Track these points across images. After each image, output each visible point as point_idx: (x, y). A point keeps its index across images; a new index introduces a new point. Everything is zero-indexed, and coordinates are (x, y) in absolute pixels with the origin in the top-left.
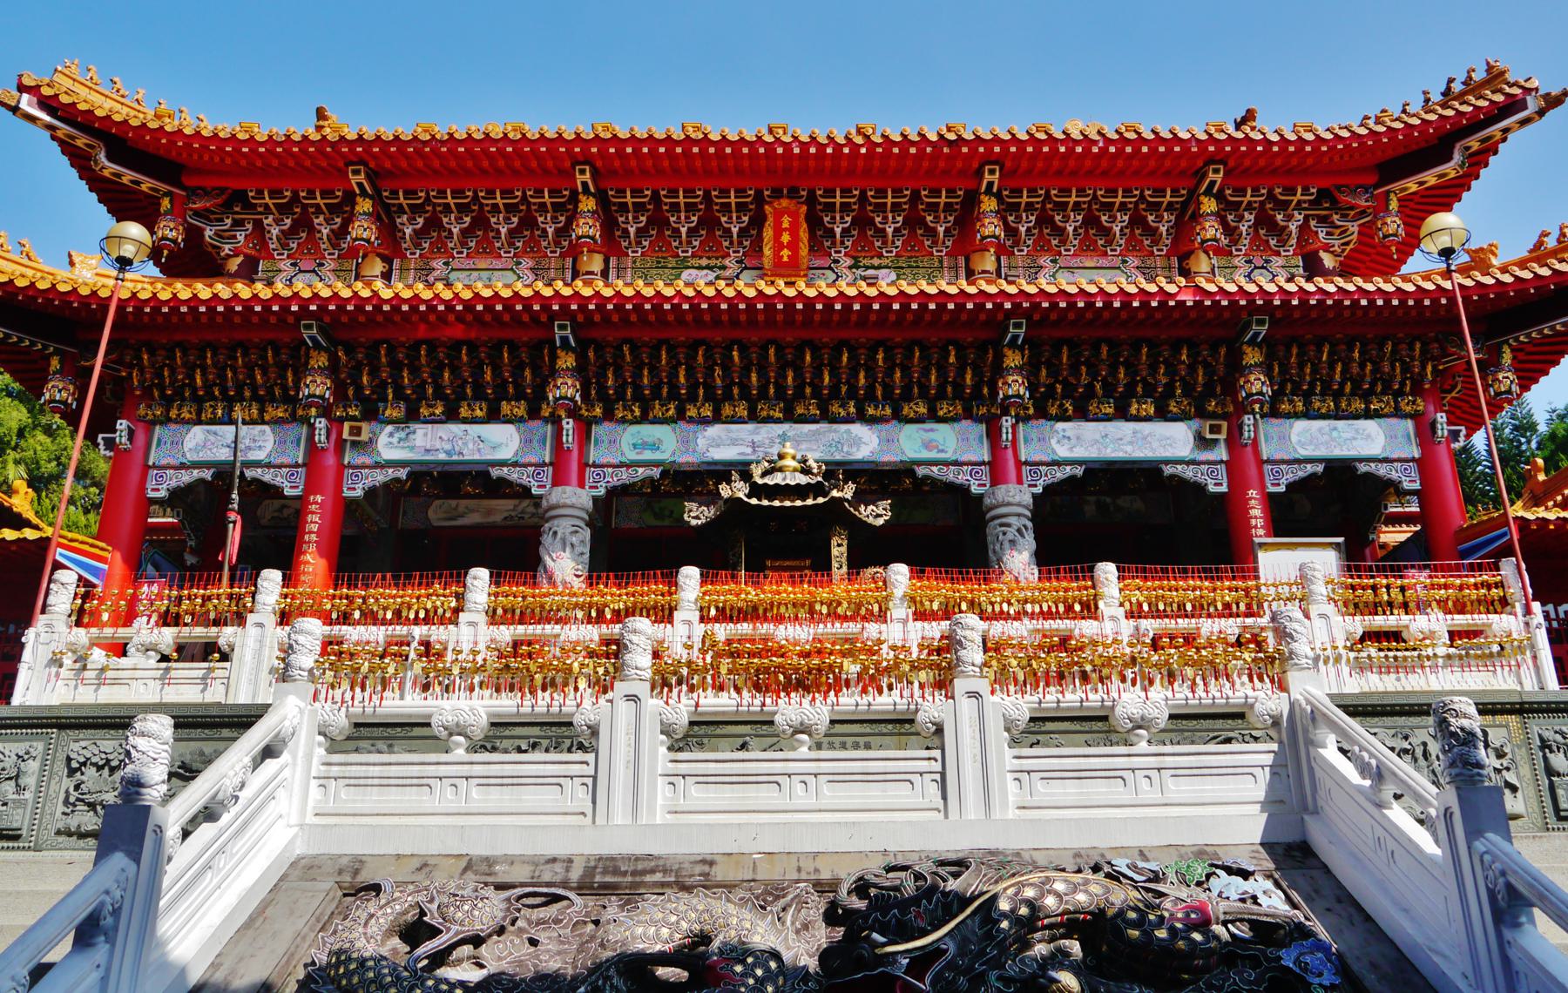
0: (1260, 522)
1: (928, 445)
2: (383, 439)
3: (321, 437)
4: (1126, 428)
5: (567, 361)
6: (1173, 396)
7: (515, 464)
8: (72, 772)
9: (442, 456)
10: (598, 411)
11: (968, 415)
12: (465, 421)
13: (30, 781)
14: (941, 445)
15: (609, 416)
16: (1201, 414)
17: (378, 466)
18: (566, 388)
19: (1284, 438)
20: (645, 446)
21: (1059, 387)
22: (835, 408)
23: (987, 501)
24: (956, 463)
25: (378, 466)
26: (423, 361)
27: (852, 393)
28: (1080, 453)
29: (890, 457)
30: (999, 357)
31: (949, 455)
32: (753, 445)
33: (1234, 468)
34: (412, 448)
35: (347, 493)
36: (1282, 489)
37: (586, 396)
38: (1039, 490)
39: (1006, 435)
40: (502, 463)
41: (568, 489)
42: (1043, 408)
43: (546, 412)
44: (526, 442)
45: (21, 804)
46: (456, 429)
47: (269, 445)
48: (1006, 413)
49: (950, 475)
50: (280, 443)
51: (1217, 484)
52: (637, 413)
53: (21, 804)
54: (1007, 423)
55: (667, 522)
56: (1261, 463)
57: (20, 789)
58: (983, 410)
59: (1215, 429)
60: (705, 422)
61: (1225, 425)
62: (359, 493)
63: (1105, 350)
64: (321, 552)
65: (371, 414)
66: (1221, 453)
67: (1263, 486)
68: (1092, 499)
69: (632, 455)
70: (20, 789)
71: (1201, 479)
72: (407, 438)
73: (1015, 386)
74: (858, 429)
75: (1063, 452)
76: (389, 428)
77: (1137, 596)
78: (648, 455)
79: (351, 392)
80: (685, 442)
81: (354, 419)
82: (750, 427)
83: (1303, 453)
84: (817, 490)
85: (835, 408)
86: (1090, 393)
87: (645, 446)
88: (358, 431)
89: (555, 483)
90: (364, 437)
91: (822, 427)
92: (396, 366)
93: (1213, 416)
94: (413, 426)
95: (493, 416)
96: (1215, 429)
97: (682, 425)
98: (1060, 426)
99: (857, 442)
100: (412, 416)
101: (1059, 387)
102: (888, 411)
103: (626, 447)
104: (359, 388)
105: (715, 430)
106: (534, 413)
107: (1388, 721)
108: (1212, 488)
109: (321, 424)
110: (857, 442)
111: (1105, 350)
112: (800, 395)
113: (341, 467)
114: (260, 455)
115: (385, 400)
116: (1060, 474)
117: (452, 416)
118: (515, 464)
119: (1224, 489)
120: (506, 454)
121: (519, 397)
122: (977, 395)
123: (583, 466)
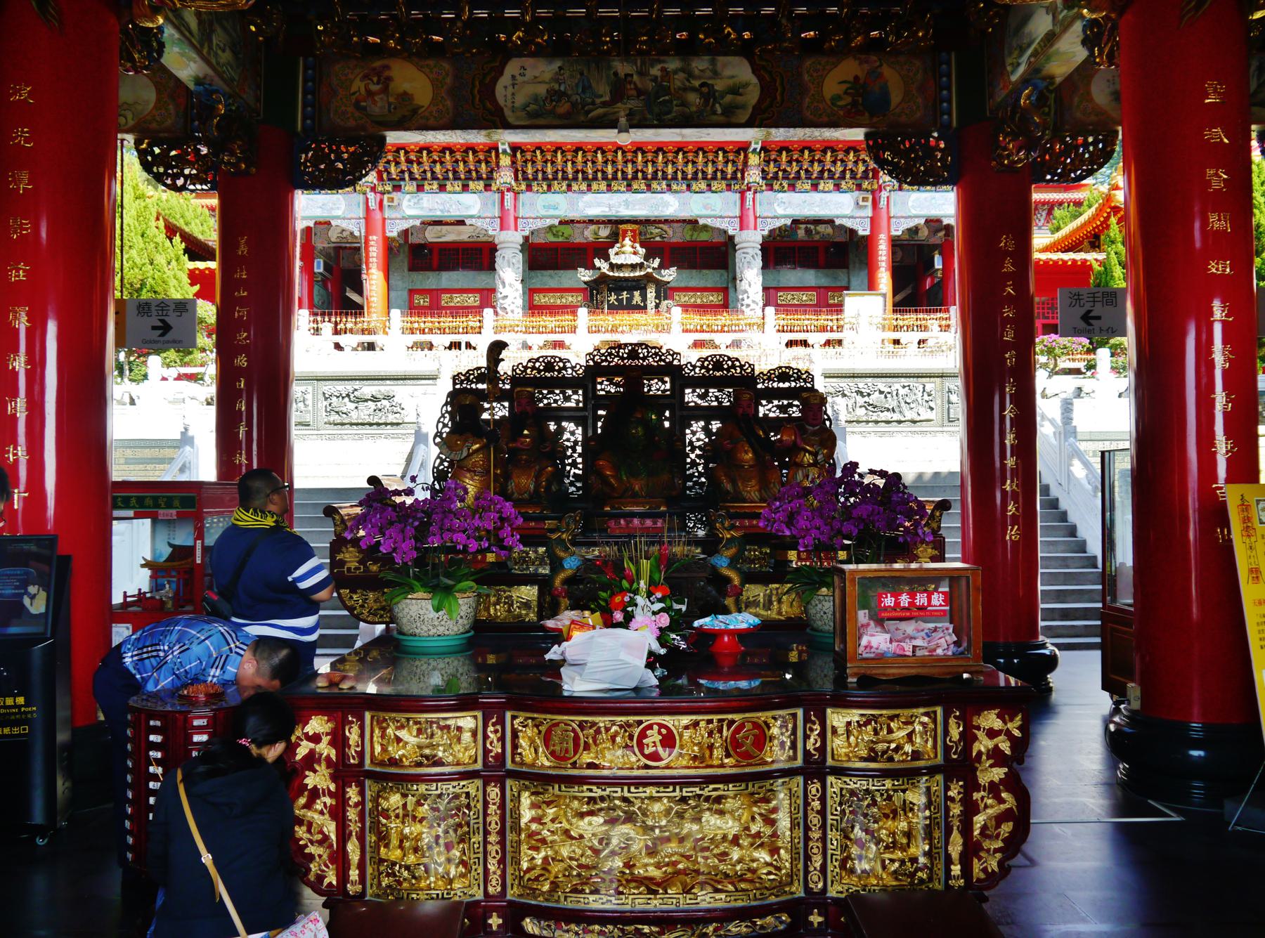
0: (884, 253)
1: (706, 207)
2: (405, 203)
3: (373, 205)
4: (816, 196)
5: (505, 161)
6: (844, 178)
7: (479, 217)
8: (326, 399)
9: (439, 213)
10: (523, 187)
11: (729, 187)
12: (450, 192)
13: (309, 402)
14: (711, 207)
15: (529, 188)
16: (859, 187)
17: (404, 218)
18: (505, 176)
19: (905, 203)
20: (549, 207)
21: (780, 174)
22: (655, 185)
23: (737, 240)
24: (721, 217)
25: (404, 218)
26: (425, 159)
27: (665, 178)
28: (790, 211)
29: (685, 214)
30: (746, 157)
31: (718, 213)
32: (610, 206)
33: (873, 220)
34: (422, 208)
35: (388, 234)
36: (899, 233)
37: (516, 179)
38: (766, 233)
39: (749, 203)
40: (472, 217)
41: (510, 232)
42: (770, 182)
43: (494, 188)
44: (484, 204)
45: (308, 412)
46: (443, 196)
47: (343, 207)
48: (749, 189)
49: (718, 224)
50: (349, 205)
51: (863, 230)
52: (545, 187)
53: (308, 412)
54: (749, 195)
55: (561, 239)
56: (889, 218)
57: (306, 406)
58: (737, 187)
59: (864, 199)
60: (582, 192)
61: (870, 197)
62: (394, 234)
63: (806, 152)
64: (378, 269)
65: (397, 188)
66: (869, 212)
67: (889, 231)
68: (803, 226)
69: (543, 212)
70: (306, 406)
71: (855, 227)
72: (418, 203)
73: (753, 176)
74: (668, 197)
75: (780, 211)
76: (408, 196)
77: (782, 323)
78: (552, 212)
79: (385, 176)
80: (572, 204)
81: (389, 192)
82: (608, 195)
83: (914, 212)
84: (641, 266)
85: (655, 185)
86: (798, 177)
87: (549, 207)
88: (392, 200)
89: (502, 229)
90: (395, 203)
91: (649, 195)
92: (409, 161)
93: (867, 190)
94: (421, 195)
95: (465, 188)
96: (864, 199)
97: (570, 194)
98: (781, 195)
99: (667, 205)
100: (420, 188)
101: (780, 174)
102: (684, 187)
103: (539, 207)
104: (389, 173)
105: (589, 197)
106: (487, 187)
107: (884, 380)
108: (861, 233)
109: (371, 196)
110: (667, 205)
111: (806, 152)
112: (635, 178)
113: (384, 220)
114: (339, 213)
115: (404, 179)
116: (778, 223)
117: (442, 188)
118: (479, 217)
119: (867, 233)
120: (474, 211)
121: (479, 178)
122: (734, 177)
123: (516, 219)
